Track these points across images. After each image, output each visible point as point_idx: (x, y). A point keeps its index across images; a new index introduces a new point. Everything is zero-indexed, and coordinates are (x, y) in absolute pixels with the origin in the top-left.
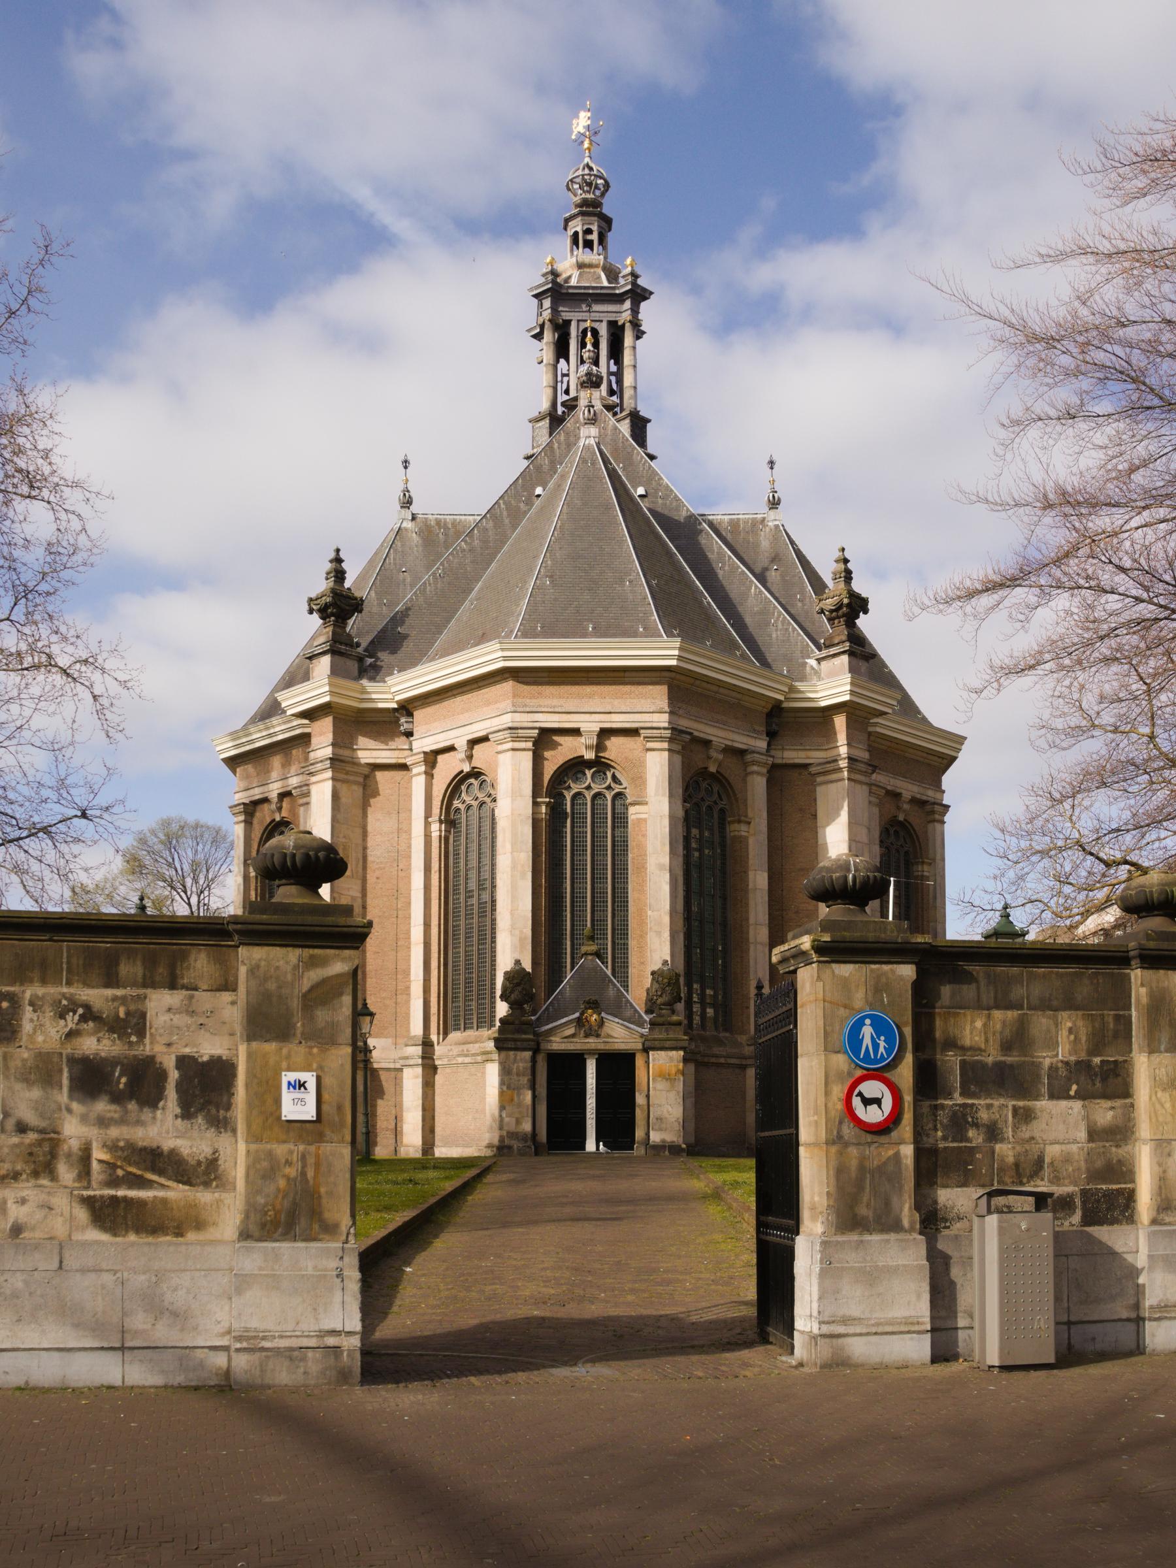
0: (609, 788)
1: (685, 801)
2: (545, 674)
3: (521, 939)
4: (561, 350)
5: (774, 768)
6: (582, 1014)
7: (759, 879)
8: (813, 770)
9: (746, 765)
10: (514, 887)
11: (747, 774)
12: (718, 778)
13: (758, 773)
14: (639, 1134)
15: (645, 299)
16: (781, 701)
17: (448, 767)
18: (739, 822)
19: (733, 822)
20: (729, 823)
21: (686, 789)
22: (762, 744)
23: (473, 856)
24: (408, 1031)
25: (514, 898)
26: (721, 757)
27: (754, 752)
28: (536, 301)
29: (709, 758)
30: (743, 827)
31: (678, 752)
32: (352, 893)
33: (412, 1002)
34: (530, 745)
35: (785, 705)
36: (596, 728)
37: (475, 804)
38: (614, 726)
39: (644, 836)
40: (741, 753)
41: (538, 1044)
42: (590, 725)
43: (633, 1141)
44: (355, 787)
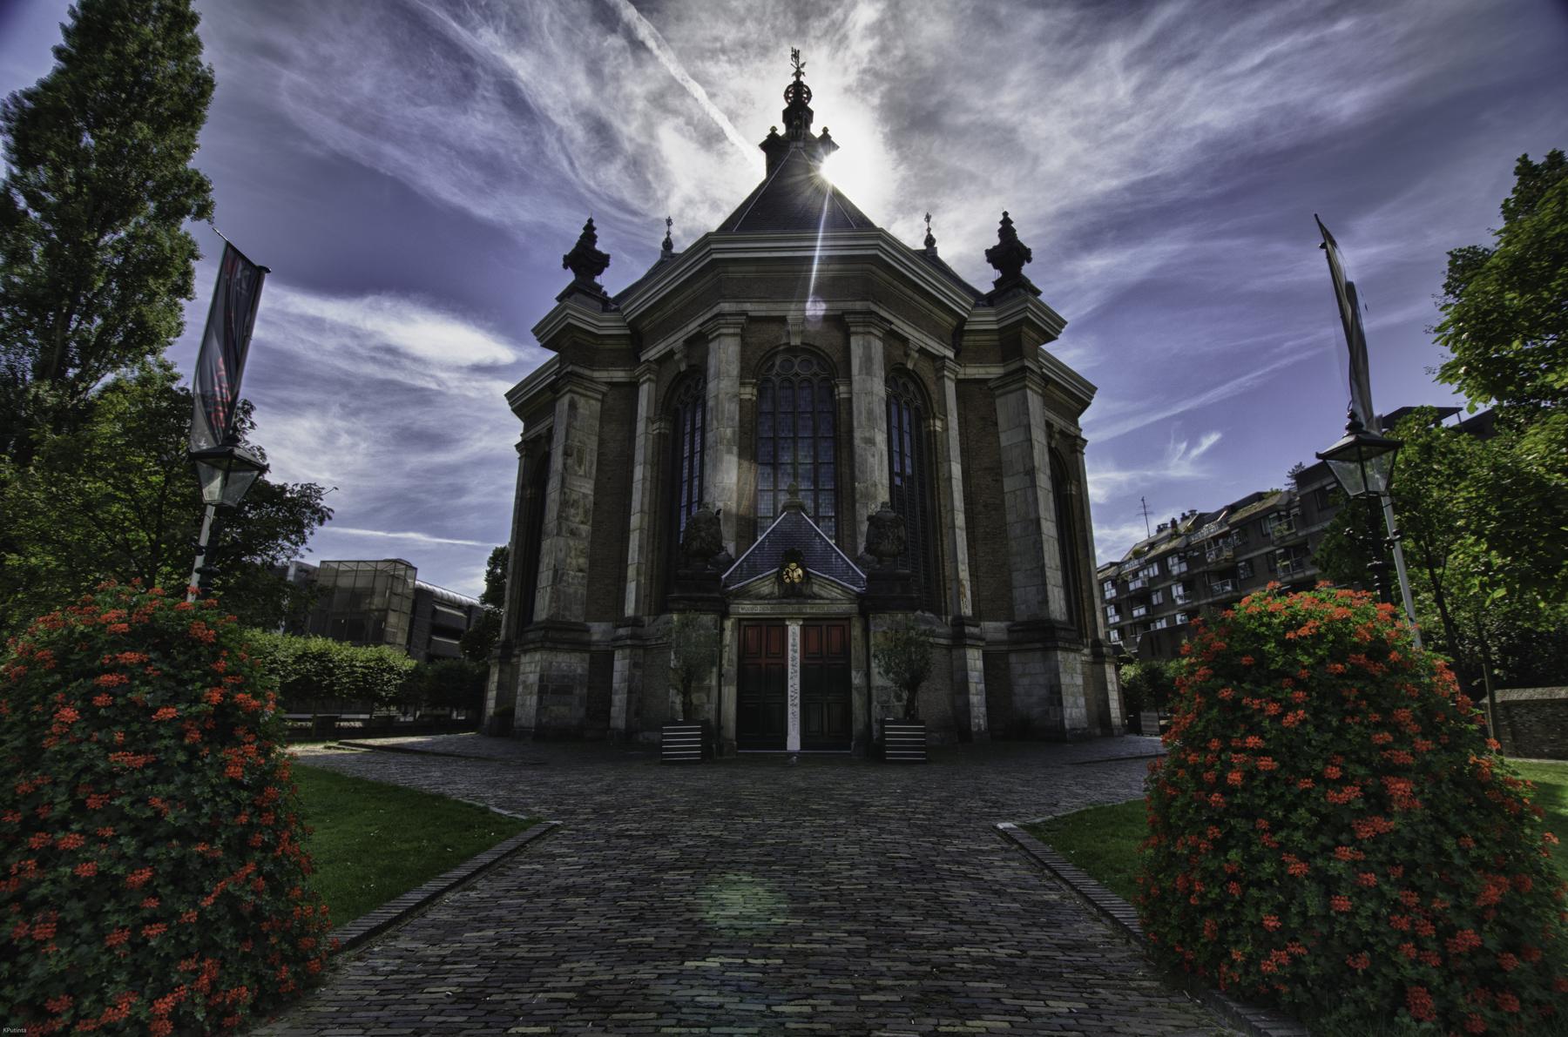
8: (991, 384)
12: (913, 376)
22: (951, 354)
40: (933, 357)
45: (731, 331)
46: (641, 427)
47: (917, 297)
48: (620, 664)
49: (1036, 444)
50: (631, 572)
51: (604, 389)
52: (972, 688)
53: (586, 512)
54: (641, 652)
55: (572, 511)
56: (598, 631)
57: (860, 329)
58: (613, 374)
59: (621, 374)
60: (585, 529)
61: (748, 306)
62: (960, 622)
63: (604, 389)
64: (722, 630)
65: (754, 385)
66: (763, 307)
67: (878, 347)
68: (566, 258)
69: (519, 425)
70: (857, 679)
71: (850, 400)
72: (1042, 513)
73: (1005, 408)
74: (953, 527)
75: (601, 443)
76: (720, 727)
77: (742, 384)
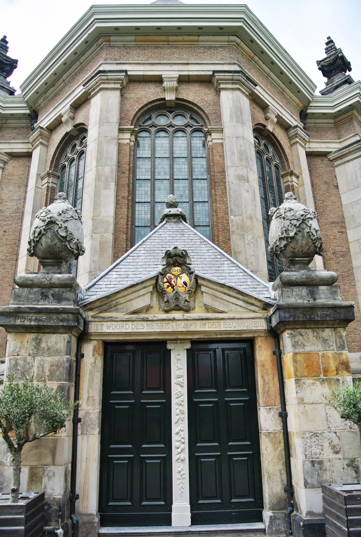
3: (101, 243)
10: (97, 195)
11: (292, 145)
14: (272, 488)
18: (292, 174)
19: (286, 175)
25: (96, 205)
29: (267, 119)
34: (118, 86)
42: (170, 72)
45: (112, 86)
63: (6, 158)
64: (80, 356)
71: (222, 144)
76: (72, 496)
77: (121, 131)
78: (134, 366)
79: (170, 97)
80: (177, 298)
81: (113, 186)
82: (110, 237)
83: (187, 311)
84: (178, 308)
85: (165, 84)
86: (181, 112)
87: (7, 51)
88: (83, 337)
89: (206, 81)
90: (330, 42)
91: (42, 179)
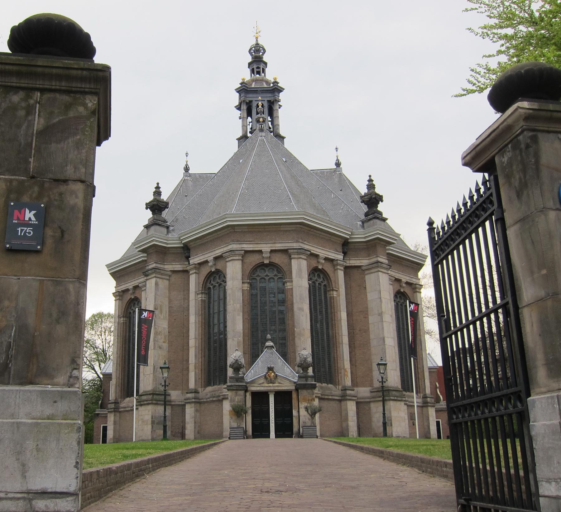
0: (276, 275)
1: (309, 280)
2: (246, 227)
4: (249, 114)
5: (346, 268)
6: (267, 373)
7: (343, 315)
8: (363, 268)
9: (334, 266)
11: (335, 270)
12: (323, 271)
13: (340, 269)
15: (281, 91)
16: (348, 239)
17: (205, 271)
18: (333, 290)
19: (330, 290)
20: (328, 291)
21: (309, 275)
22: (340, 257)
23: (216, 308)
24: (188, 387)
26: (323, 261)
27: (337, 260)
28: (238, 94)
29: (318, 262)
30: (335, 293)
31: (305, 259)
32: (163, 326)
33: (190, 374)
34: (240, 258)
35: (350, 241)
36: (269, 250)
37: (217, 285)
38: (277, 248)
39: (292, 296)
41: (247, 388)
42: (266, 248)
43: (292, 434)
44: (165, 281)
45: (237, 258)
46: (192, 296)
47: (322, 233)
48: (190, 411)
49: (383, 300)
50: (192, 367)
51: (170, 273)
52: (350, 419)
53: (165, 337)
54: (198, 405)
55: (159, 337)
56: (175, 395)
57: (296, 256)
58: (174, 266)
59: (179, 266)
60: (165, 345)
61: (244, 246)
62: (345, 389)
63: (170, 273)
64: (245, 396)
65: (248, 283)
66: (251, 246)
67: (304, 263)
68: (147, 204)
69: (113, 283)
70: (295, 413)
71: (292, 289)
72: (386, 335)
73: (370, 279)
74: (342, 344)
75: (170, 301)
78: (260, 398)
79: (266, 262)
80: (271, 379)
81: (241, 314)
82: (241, 339)
83: (274, 383)
84: (271, 383)
85: (264, 255)
86: (272, 267)
87: (161, 195)
88: (246, 391)
89: (285, 251)
90: (370, 180)
91: (198, 294)
